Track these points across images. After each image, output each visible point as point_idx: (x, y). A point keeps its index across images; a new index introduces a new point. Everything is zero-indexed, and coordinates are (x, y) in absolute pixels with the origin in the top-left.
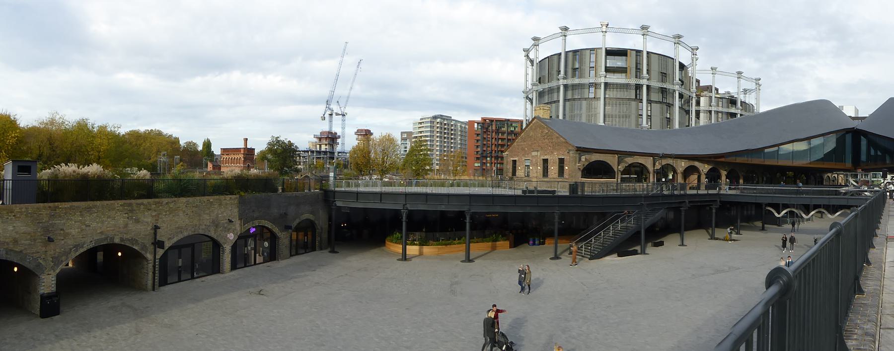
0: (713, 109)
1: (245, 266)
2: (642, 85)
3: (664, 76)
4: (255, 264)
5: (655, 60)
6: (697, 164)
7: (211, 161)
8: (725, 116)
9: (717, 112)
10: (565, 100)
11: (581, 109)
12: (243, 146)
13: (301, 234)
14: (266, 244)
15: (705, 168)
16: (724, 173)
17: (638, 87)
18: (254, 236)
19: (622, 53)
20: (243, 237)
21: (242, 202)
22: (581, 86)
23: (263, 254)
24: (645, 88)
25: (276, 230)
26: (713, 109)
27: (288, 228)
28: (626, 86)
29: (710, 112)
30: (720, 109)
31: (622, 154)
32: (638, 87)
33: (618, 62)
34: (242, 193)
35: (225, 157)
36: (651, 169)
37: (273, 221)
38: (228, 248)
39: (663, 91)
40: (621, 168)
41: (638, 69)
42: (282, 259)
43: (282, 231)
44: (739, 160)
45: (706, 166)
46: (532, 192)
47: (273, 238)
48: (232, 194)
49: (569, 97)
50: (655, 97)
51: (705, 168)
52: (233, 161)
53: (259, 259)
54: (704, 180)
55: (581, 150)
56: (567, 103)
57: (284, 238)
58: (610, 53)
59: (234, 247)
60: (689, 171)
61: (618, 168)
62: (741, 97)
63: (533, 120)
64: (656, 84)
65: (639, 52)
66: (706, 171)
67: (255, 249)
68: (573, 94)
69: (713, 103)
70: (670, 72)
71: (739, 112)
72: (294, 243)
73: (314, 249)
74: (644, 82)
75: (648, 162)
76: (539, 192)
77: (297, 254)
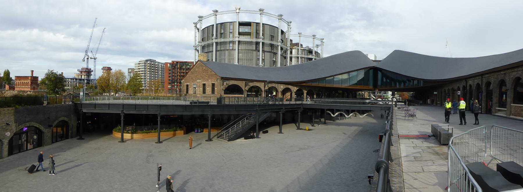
0: (300, 56)
1: (20, 152)
3: (272, 37)
4: (27, 150)
5: (267, 29)
6: (290, 87)
7: (9, 84)
8: (306, 60)
9: (302, 58)
10: (216, 51)
11: (225, 55)
12: (30, 75)
13: (59, 130)
14: (35, 137)
15: (294, 89)
16: (305, 92)
17: (257, 43)
18: (26, 132)
19: (248, 24)
20: (18, 134)
21: (17, 112)
22: (225, 43)
23: (33, 143)
24: (261, 44)
25: (42, 128)
27: (50, 126)
28: (250, 43)
29: (298, 57)
30: (303, 56)
31: (247, 81)
32: (257, 43)
33: (245, 29)
34: (17, 106)
35: (18, 81)
36: (263, 89)
37: (40, 123)
38: (6, 142)
39: (272, 46)
40: (247, 88)
41: (257, 33)
42: (46, 145)
43: (46, 128)
44: (314, 84)
45: (295, 88)
46: (196, 103)
47: (39, 133)
48: (9, 106)
49: (219, 49)
50: (267, 49)
51: (294, 89)
52: (23, 84)
53: (30, 146)
54: (294, 96)
55: (224, 79)
57: (47, 133)
58: (241, 24)
59: (11, 141)
61: (245, 88)
62: (315, 49)
64: (267, 41)
65: (258, 24)
66: (295, 90)
67: (27, 141)
69: (300, 53)
70: (275, 35)
71: (314, 57)
72: (55, 135)
73: (67, 138)
74: (261, 40)
75: (261, 85)
76: (200, 103)
77: (57, 141)
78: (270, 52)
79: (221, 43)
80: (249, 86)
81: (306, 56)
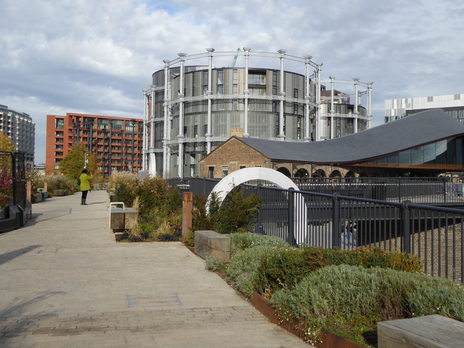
0: (332, 115)
2: (279, 101)
3: (295, 92)
9: (336, 118)
10: (212, 112)
11: (226, 120)
15: (344, 172)
16: (357, 175)
19: (262, 72)
22: (226, 101)
24: (282, 103)
26: (332, 115)
28: (265, 102)
29: (329, 118)
30: (338, 115)
32: (276, 103)
40: (295, 171)
41: (276, 88)
45: (345, 170)
49: (215, 109)
50: (290, 110)
51: (344, 172)
56: (213, 115)
58: (252, 72)
60: (335, 173)
63: (231, 138)
64: (290, 99)
66: (345, 174)
68: (217, 107)
69: (332, 110)
70: (300, 88)
71: (356, 116)
74: (281, 98)
75: (308, 167)
78: (293, 115)
79: (217, 100)
80: (297, 168)
81: (343, 116)
